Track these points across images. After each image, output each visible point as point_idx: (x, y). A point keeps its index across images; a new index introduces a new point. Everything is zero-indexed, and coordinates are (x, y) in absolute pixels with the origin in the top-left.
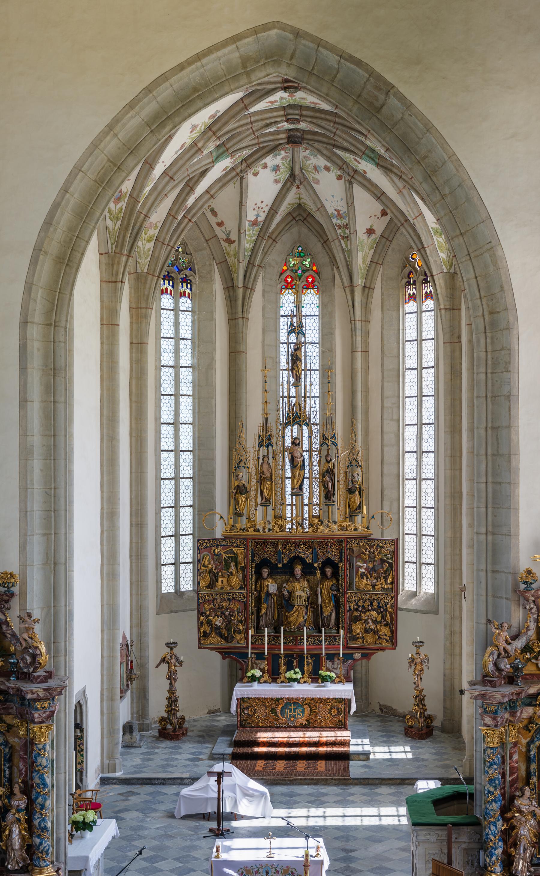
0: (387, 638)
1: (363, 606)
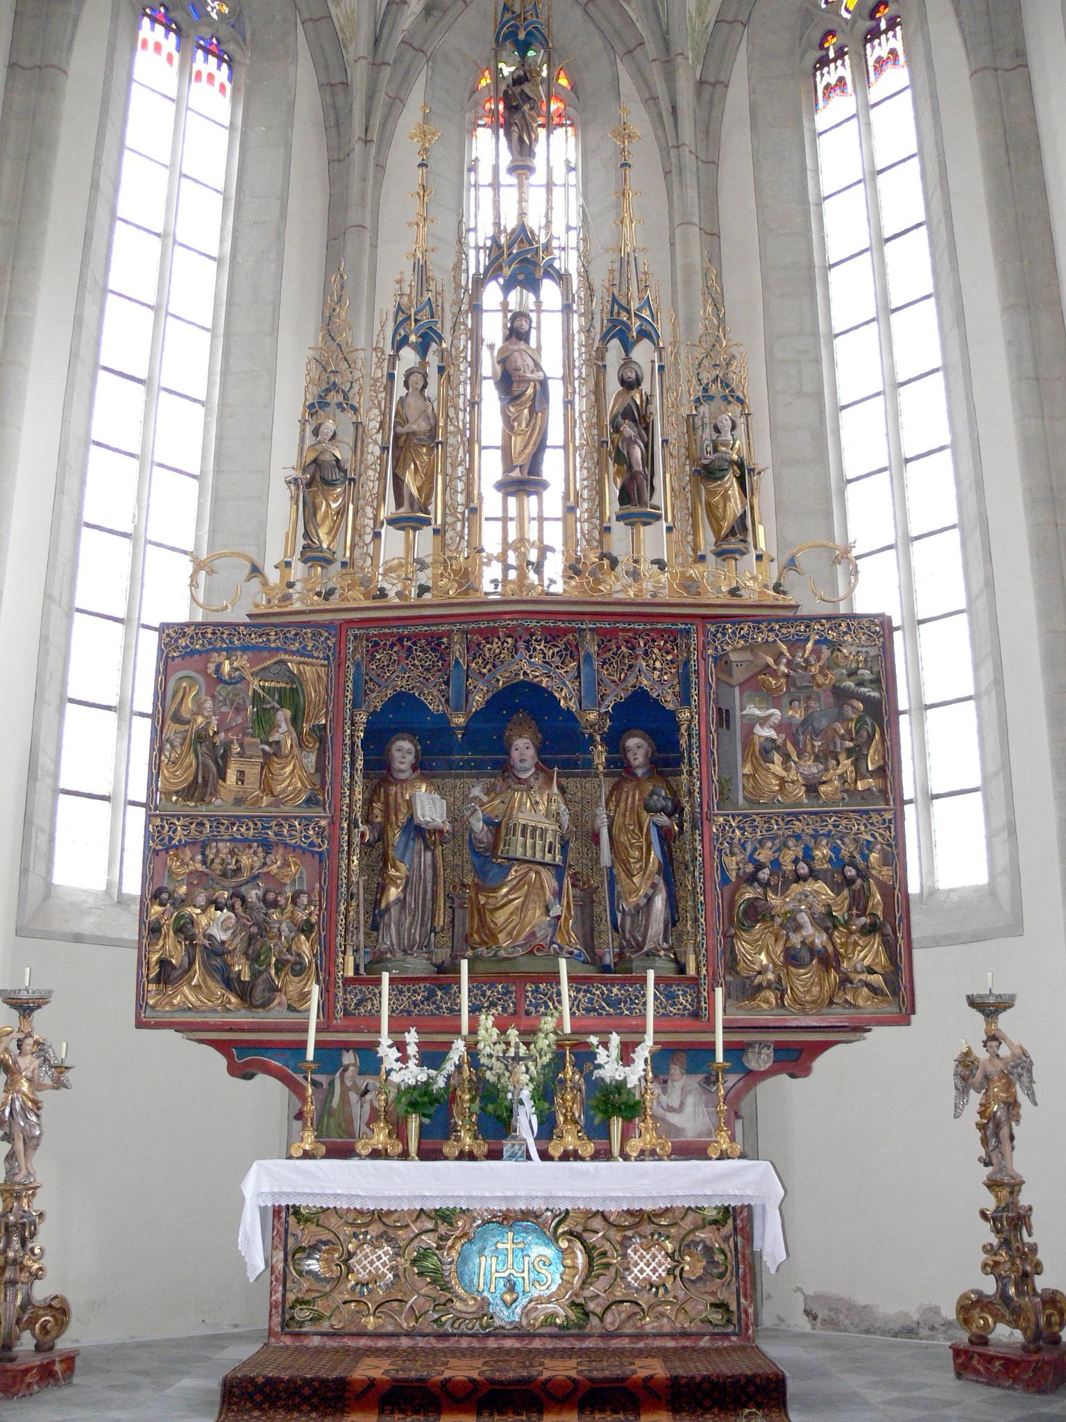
0: (877, 979)
1: (776, 864)
